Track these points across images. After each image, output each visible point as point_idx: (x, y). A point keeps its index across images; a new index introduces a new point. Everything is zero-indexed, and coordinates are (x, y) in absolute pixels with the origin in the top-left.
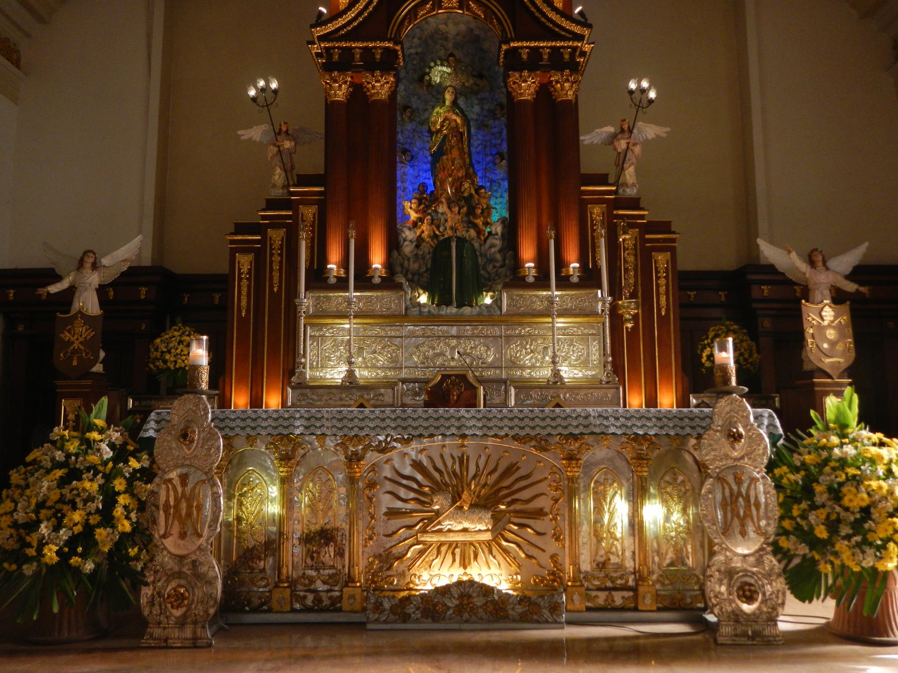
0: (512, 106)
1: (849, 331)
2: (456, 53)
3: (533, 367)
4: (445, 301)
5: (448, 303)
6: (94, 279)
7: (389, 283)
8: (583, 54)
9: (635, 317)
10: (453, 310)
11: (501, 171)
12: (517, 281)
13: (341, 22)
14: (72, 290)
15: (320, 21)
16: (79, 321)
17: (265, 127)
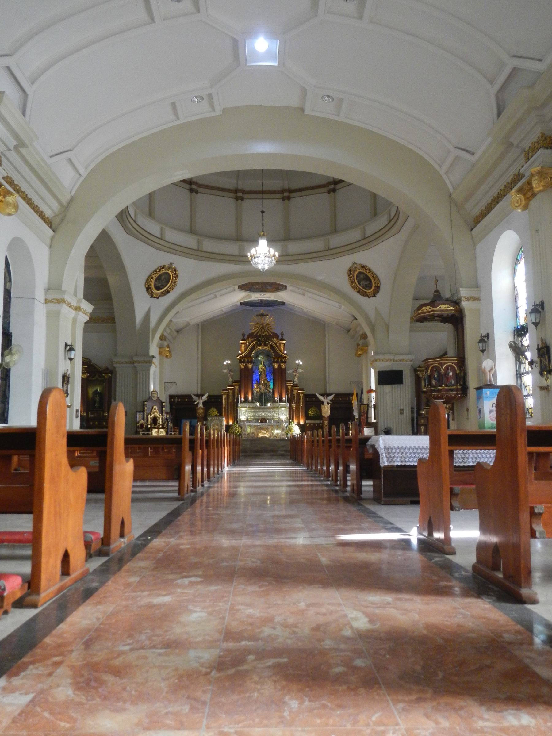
0: (273, 368)
1: (329, 410)
2: (264, 352)
3: (277, 416)
4: (262, 405)
5: (262, 405)
6: (202, 401)
7: (252, 402)
8: (287, 358)
9: (295, 407)
10: (263, 407)
11: (272, 376)
12: (274, 401)
13: (242, 355)
14: (198, 404)
15: (239, 354)
16: (201, 409)
17: (228, 370)
